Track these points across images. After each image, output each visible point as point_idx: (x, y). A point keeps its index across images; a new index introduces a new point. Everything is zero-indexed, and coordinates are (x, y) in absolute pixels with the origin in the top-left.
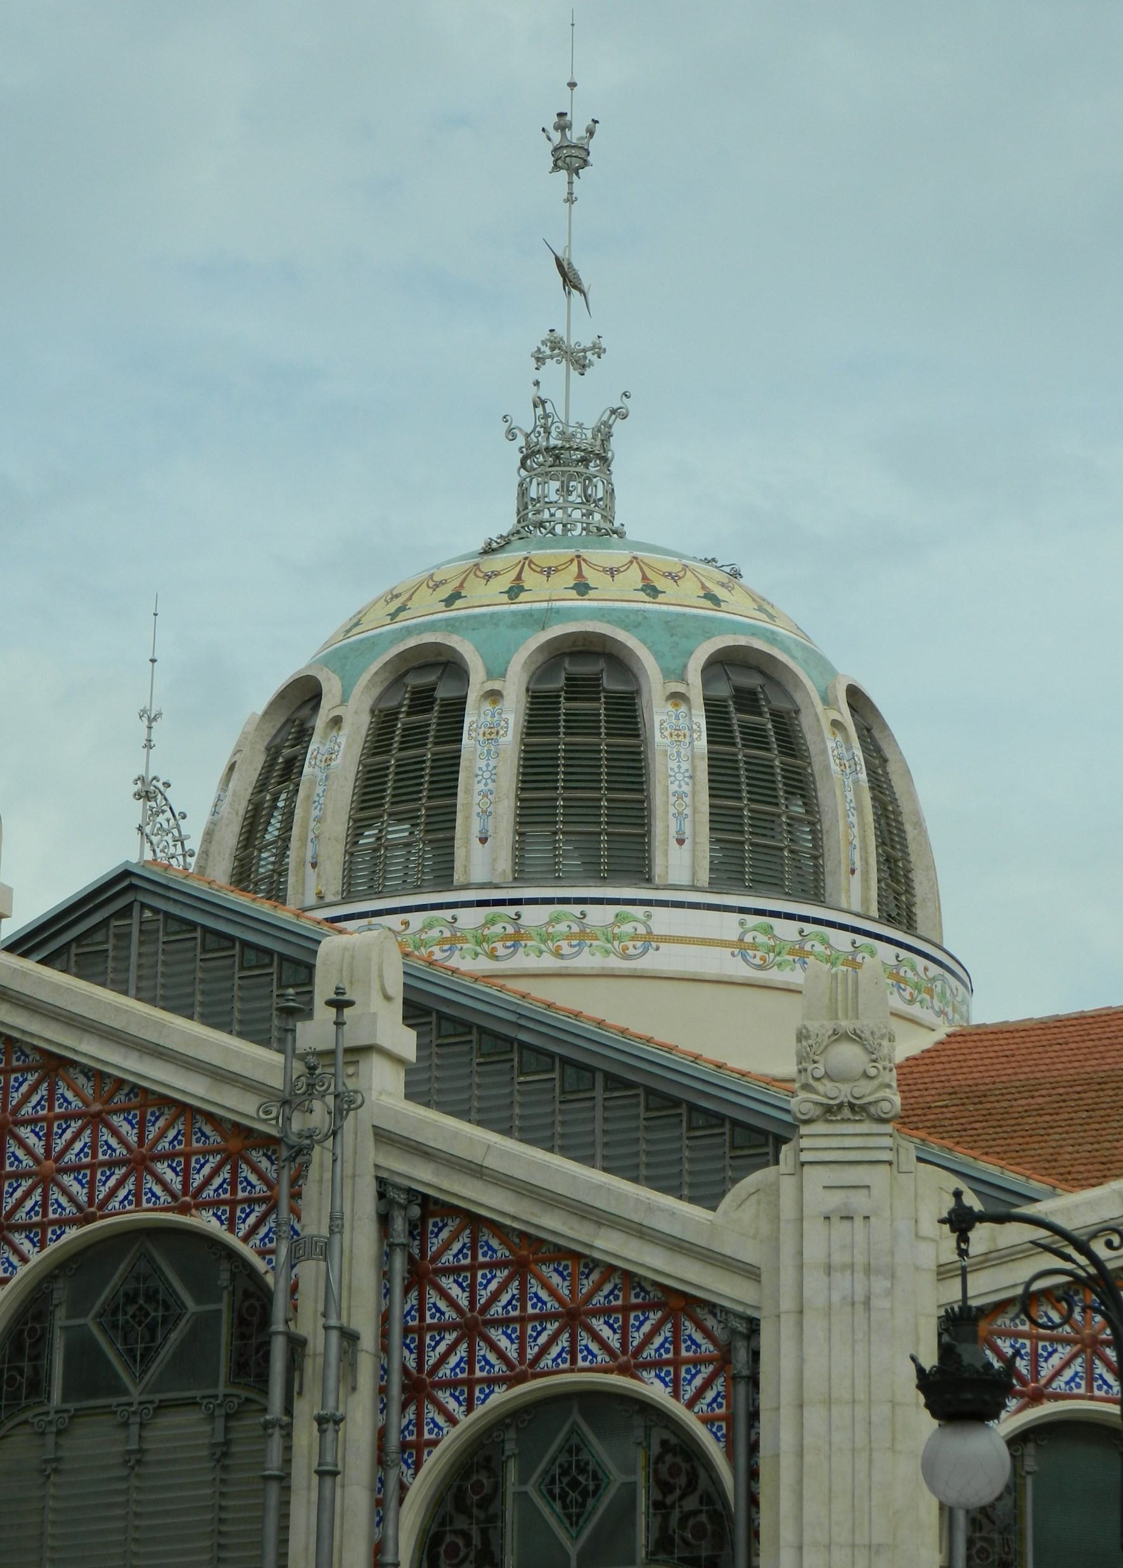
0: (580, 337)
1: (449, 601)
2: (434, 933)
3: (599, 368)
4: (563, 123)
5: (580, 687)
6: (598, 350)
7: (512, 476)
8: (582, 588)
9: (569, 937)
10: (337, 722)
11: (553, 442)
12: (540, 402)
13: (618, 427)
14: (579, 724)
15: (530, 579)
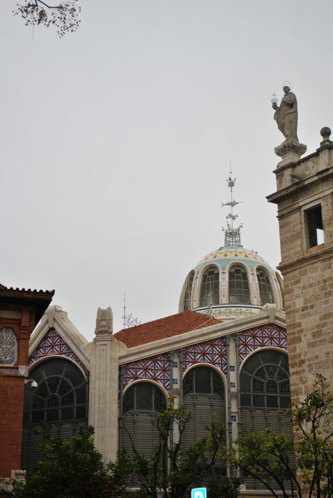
0: (234, 214)
1: (215, 257)
2: (217, 312)
3: (237, 219)
4: (230, 179)
5: (238, 271)
6: (237, 216)
7: (224, 237)
8: (236, 255)
9: (239, 313)
10: (197, 277)
11: (231, 232)
12: (228, 225)
13: (241, 228)
14: (238, 277)
15: (228, 254)
